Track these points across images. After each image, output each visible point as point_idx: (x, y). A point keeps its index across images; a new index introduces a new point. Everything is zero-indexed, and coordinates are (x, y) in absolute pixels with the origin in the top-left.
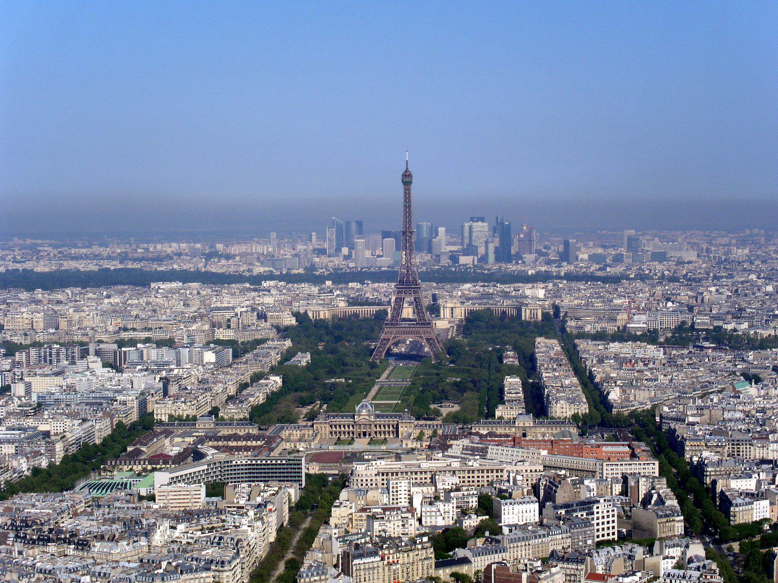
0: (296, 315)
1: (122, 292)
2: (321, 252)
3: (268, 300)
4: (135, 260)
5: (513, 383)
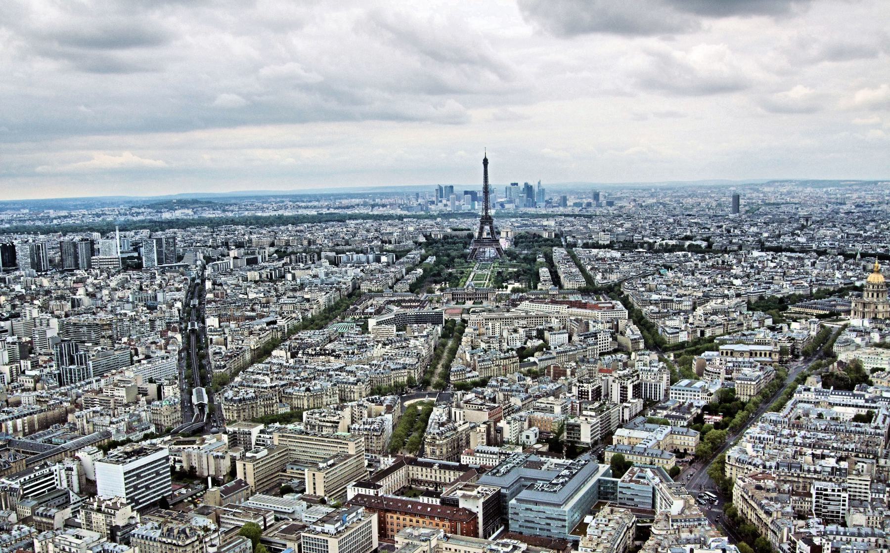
0: (425, 236)
1: (333, 226)
2: (433, 203)
3: (411, 229)
4: (335, 208)
5: (544, 272)
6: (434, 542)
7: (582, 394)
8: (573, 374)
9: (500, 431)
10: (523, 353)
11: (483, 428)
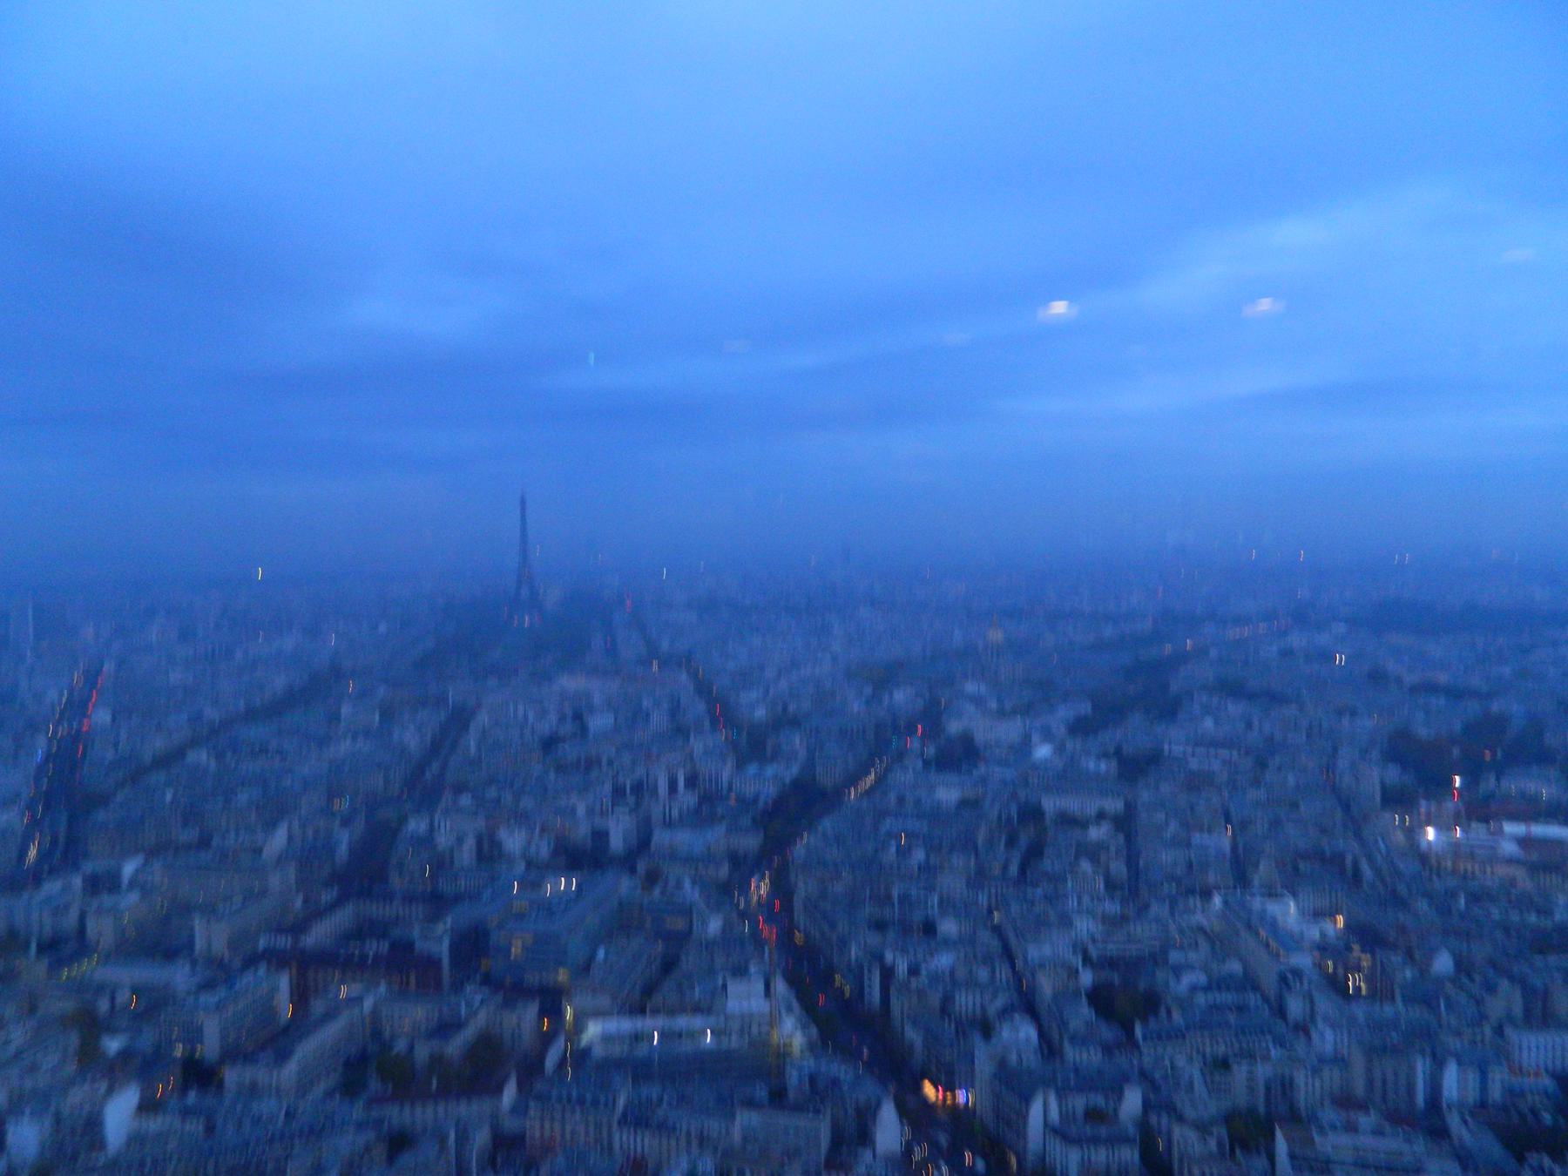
6: (368, 1004)
7: (618, 792)
8: (610, 763)
9: (496, 844)
10: (550, 743)
11: (470, 844)
